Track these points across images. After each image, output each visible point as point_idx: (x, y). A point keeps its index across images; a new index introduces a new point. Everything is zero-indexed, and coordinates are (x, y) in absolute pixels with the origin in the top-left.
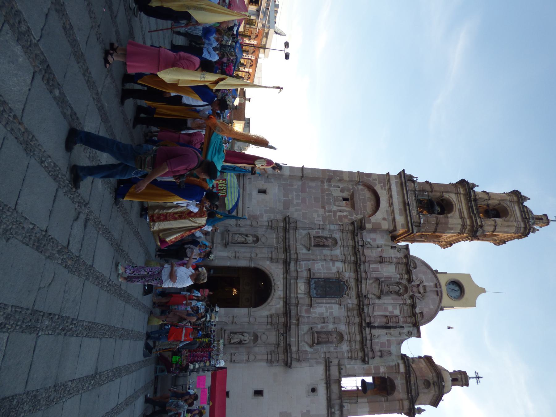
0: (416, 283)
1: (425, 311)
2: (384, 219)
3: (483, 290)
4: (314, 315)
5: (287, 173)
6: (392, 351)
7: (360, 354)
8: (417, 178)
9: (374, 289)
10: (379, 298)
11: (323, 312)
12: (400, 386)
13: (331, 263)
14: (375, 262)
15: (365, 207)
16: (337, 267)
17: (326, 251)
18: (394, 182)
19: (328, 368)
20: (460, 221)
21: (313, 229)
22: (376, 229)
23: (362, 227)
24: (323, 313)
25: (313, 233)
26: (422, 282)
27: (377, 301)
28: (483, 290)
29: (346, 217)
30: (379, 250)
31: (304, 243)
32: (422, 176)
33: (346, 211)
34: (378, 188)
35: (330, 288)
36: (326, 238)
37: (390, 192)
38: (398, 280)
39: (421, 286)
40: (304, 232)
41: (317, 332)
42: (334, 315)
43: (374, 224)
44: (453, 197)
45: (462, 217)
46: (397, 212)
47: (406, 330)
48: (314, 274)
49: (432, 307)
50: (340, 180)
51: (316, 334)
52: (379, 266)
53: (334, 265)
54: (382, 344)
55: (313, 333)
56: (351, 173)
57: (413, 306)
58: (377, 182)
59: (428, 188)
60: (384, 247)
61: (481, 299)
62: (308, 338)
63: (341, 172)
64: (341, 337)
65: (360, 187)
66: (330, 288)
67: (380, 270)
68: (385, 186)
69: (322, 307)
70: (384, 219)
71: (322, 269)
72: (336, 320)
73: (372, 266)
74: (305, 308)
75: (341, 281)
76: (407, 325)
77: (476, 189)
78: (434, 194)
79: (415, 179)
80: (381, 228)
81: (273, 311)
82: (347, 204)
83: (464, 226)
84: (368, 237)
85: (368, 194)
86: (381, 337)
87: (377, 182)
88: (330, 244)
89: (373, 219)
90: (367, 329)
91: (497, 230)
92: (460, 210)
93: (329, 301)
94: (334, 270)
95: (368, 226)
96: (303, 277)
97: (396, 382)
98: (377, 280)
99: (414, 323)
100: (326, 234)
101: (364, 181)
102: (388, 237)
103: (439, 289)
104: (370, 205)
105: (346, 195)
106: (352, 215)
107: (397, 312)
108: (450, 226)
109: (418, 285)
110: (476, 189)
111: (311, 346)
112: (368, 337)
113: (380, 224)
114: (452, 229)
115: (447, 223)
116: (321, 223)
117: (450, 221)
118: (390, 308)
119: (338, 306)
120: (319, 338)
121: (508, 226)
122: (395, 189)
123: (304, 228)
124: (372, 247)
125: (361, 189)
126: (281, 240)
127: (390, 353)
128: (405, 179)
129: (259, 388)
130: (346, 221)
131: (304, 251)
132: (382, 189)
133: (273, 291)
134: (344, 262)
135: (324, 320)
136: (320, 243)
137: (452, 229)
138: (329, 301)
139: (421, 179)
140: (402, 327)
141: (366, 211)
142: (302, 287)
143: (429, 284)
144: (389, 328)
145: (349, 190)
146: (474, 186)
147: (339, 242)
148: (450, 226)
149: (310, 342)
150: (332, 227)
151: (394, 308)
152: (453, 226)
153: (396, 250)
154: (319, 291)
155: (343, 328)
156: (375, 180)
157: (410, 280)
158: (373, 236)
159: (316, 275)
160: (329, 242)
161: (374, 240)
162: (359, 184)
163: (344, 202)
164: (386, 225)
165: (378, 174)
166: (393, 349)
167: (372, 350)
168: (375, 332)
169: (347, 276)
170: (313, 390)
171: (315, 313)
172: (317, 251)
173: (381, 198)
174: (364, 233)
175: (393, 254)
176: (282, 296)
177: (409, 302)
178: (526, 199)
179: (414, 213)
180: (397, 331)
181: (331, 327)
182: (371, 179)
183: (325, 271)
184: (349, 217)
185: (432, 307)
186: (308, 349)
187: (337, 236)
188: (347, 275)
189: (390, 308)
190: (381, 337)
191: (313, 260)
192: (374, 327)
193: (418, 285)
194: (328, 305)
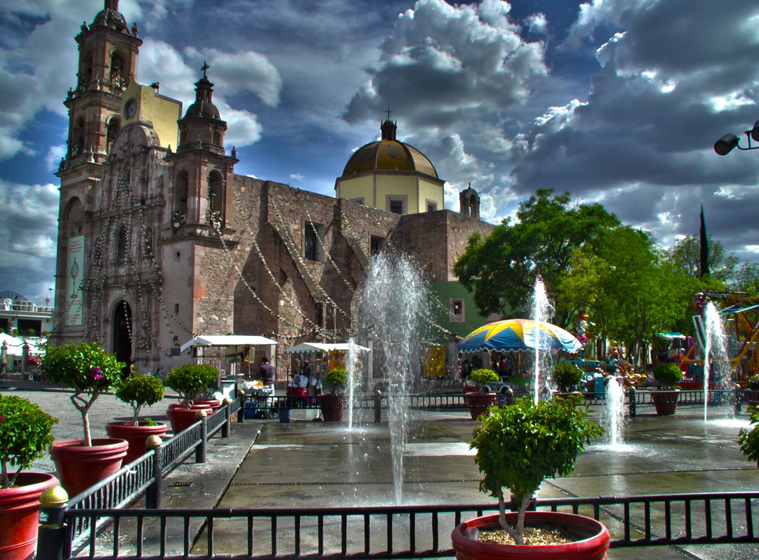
1: (140, 141)
34: (68, 199)
45: (84, 108)
64: (149, 230)
65: (70, 217)
90: (148, 202)
97: (180, 169)
103: (127, 129)
114: (95, 116)
122: (70, 182)
124: (102, 201)
127: (162, 177)
129: (173, 308)
148: (91, 120)
157: (121, 161)
158: (97, 200)
162: (68, 217)
166: (160, 173)
170: (179, 255)
180: (150, 171)
192: (147, 194)
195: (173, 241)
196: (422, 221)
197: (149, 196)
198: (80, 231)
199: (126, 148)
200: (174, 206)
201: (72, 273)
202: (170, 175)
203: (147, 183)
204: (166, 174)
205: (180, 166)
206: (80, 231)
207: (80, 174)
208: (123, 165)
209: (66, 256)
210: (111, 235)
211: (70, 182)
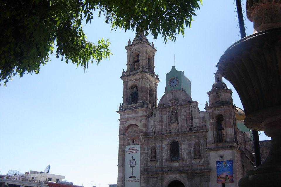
0: (170, 103)
1: (183, 98)
2: (141, 122)
3: (173, 67)
4: (187, 158)
5: (121, 174)
6: (203, 116)
7: (204, 133)
8: (121, 104)
9: (174, 125)
10: (178, 123)
11: (186, 153)
12: (218, 111)
13: (164, 149)
14: (162, 126)
15: (137, 131)
16: (166, 145)
17: (158, 153)
18: (123, 116)
19: (211, 150)
20: (141, 80)
21: (148, 158)
22: (146, 126)
23: (146, 134)
24: (186, 153)
25: (149, 159)
26: (170, 101)
27: (180, 124)
28: (173, 67)
29: (141, 142)
30: (156, 123)
31: (154, 164)
32: (120, 100)
33: (139, 142)
35: (175, 149)
36: (151, 152)
37: (128, 119)
38: (170, 113)
39: (172, 101)
40: (149, 164)
41: (195, 156)
42: (187, 147)
43: (143, 127)
44: (130, 84)
45: (138, 79)
46: (137, 115)
47: (193, 109)
48: (168, 159)
49: (182, 95)
50: (124, 145)
51: (195, 157)
52: (164, 123)
53: (164, 148)
54: (200, 121)
55: (195, 158)
56: (120, 140)
57: (182, 105)
58: (124, 126)
59: (125, 97)
60: (155, 121)
61: (178, 69)
62: (198, 161)
63: (120, 145)
65: (127, 134)
66: (175, 149)
67: (166, 123)
68: (125, 121)
69: (184, 154)
70: (141, 122)
71: (166, 155)
72: (190, 146)
73: (164, 128)
74: (184, 163)
75: (171, 144)
76: (190, 108)
77: (125, 71)
78: (128, 94)
79: (122, 105)
80: (145, 123)
81: (186, 179)
82: (136, 141)
83: (143, 78)
84: (151, 129)
85: (130, 130)
86: (196, 122)
87: (124, 126)
88: (154, 150)
89: (141, 128)
91: (145, 58)
92: (136, 80)
93: (180, 150)
94: (166, 148)
95: (144, 130)
96: (170, 164)
98: (169, 125)
99: (190, 103)
100: (149, 152)
101: (123, 132)
102: (150, 119)
104: (135, 129)
105: (131, 142)
106: (140, 139)
107: (185, 114)
108: (143, 86)
109: (172, 102)
110: (125, 71)
111: (201, 158)
112: (196, 129)
113: (143, 124)
114: (145, 84)
115: (142, 87)
116: (144, 155)
117: (140, 86)
118: (183, 117)
119: (183, 145)
120: (198, 154)
121: (143, 53)
122: (126, 116)
123: (147, 164)
124: (155, 127)
125: (127, 135)
126: (153, 176)
127: (204, 117)
128: (122, 110)
130: (143, 141)
131: (158, 164)
132: (127, 123)
133: (177, 180)
134: (162, 143)
135: (189, 153)
136: (154, 156)
137: (145, 84)
138: (180, 150)
139: (121, 101)
140: (192, 110)
141: (138, 131)
142: (175, 164)
143: (171, 96)
144: (192, 117)
145: (128, 140)
146: (124, 72)
147: (153, 145)
148: (143, 86)
149: (199, 160)
150: (146, 149)
151: (183, 115)
152: (143, 84)
153: (156, 114)
154: (177, 155)
155: (193, 142)
156: (122, 127)
158: (150, 127)
159: (169, 158)
160: (153, 151)
161: (152, 126)
163: (135, 142)
164: (144, 121)
165: (120, 125)
166: (202, 115)
167: (202, 127)
168: (194, 125)
169: (169, 141)
171: (186, 157)
172: (158, 157)
173: (131, 124)
174: (149, 131)
175: (158, 115)
176: (179, 175)
177: (179, 107)
178: (129, 42)
179: (137, 105)
180: (193, 113)
181: (192, 149)
182: (122, 129)
183: (167, 152)
184: (141, 140)
185: (182, 95)
186: (202, 161)
187: (150, 146)
188: (168, 141)
189: (183, 117)
190: (196, 122)
191: (162, 159)
192: (192, 125)
193: (172, 102)
194: (183, 151)
195: (217, 149)
196: (265, 144)
197: (194, 126)
198: (133, 142)
199: (173, 101)
200: (215, 132)
201: (130, 164)
202: (210, 116)
203: (192, 119)
204: (207, 116)
205: (217, 112)
206: (133, 142)
207: (138, 112)
208: (171, 109)
209: (125, 155)
210: (164, 145)
211: (126, 116)
